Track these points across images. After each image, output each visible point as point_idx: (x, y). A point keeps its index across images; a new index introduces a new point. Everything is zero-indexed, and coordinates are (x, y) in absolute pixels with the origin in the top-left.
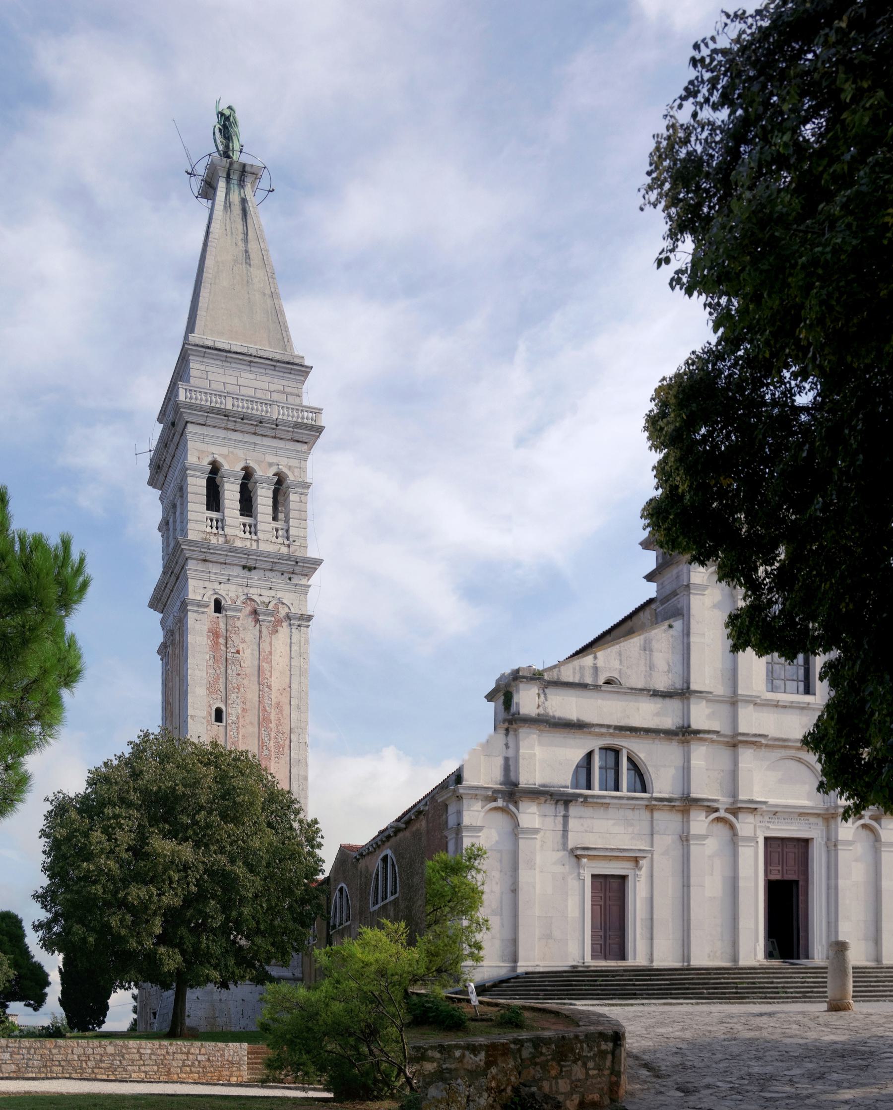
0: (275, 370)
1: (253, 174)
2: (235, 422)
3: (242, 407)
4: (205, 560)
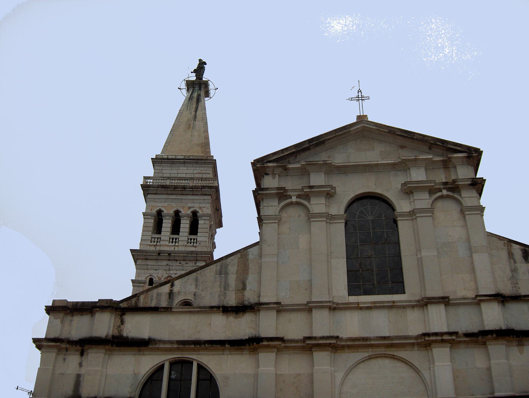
0: (197, 164)
1: (205, 84)
2: (171, 190)
3: (175, 182)
4: (146, 259)
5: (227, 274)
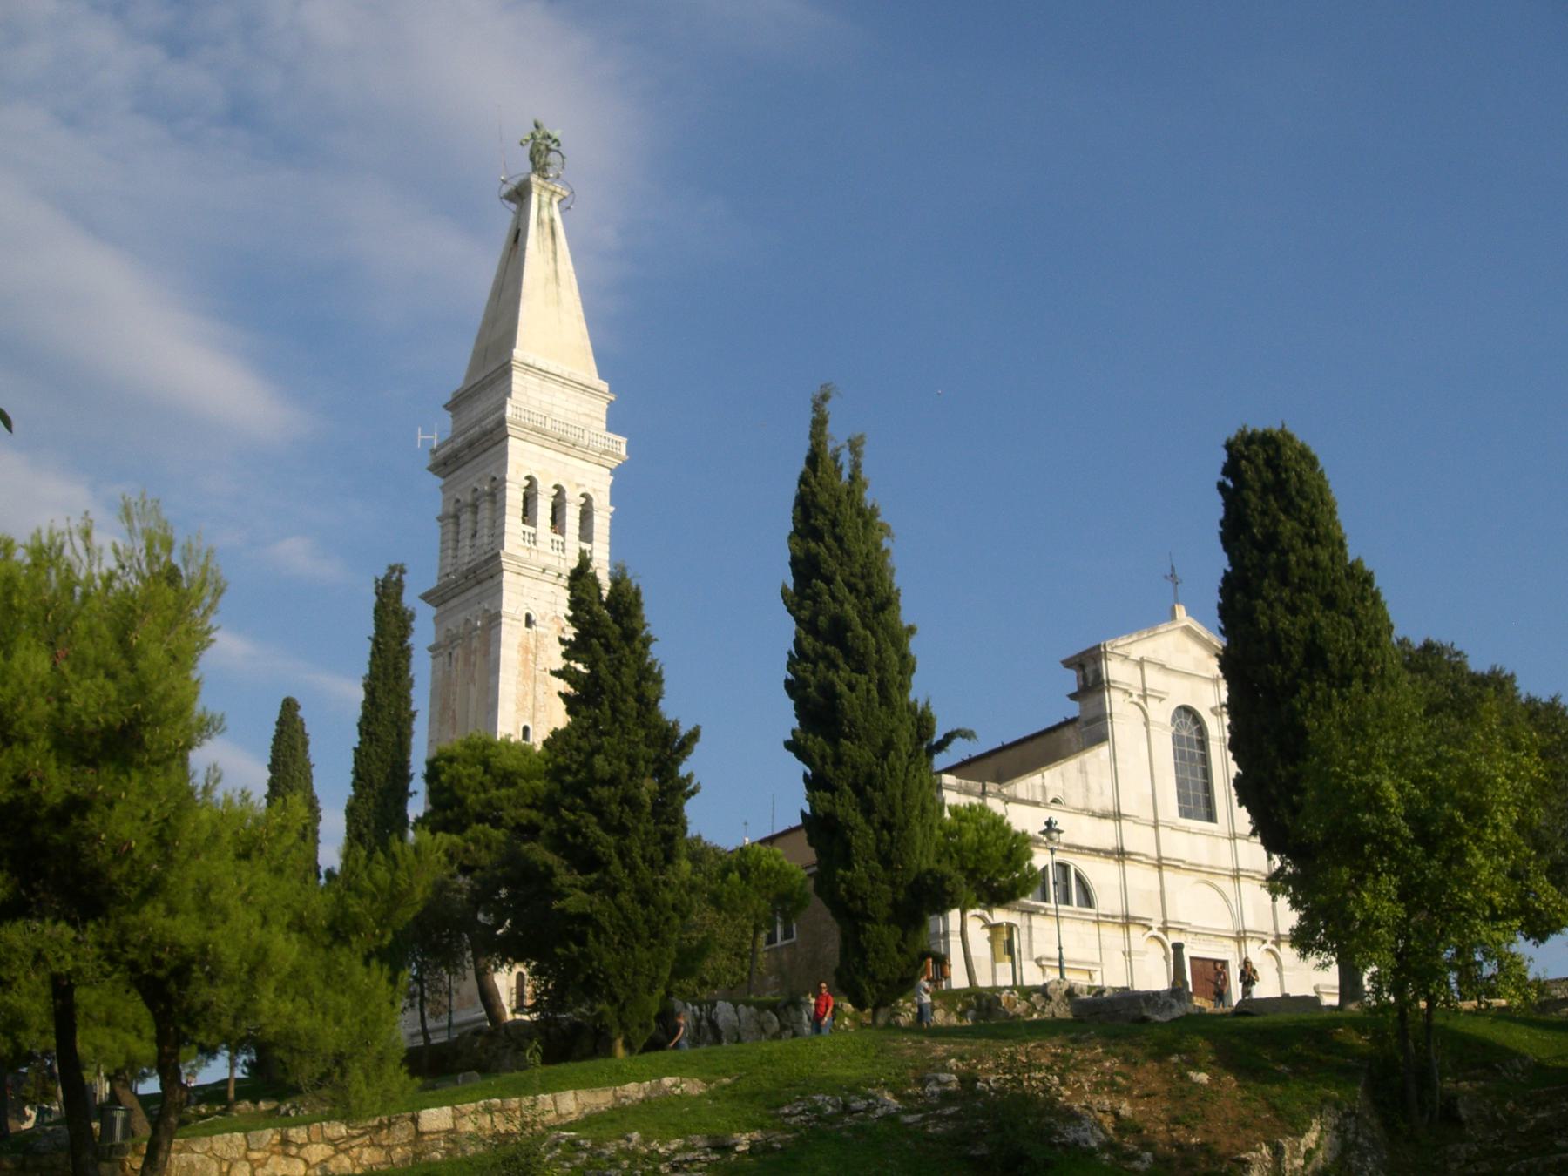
4: (519, 574)
5: (1086, 773)
